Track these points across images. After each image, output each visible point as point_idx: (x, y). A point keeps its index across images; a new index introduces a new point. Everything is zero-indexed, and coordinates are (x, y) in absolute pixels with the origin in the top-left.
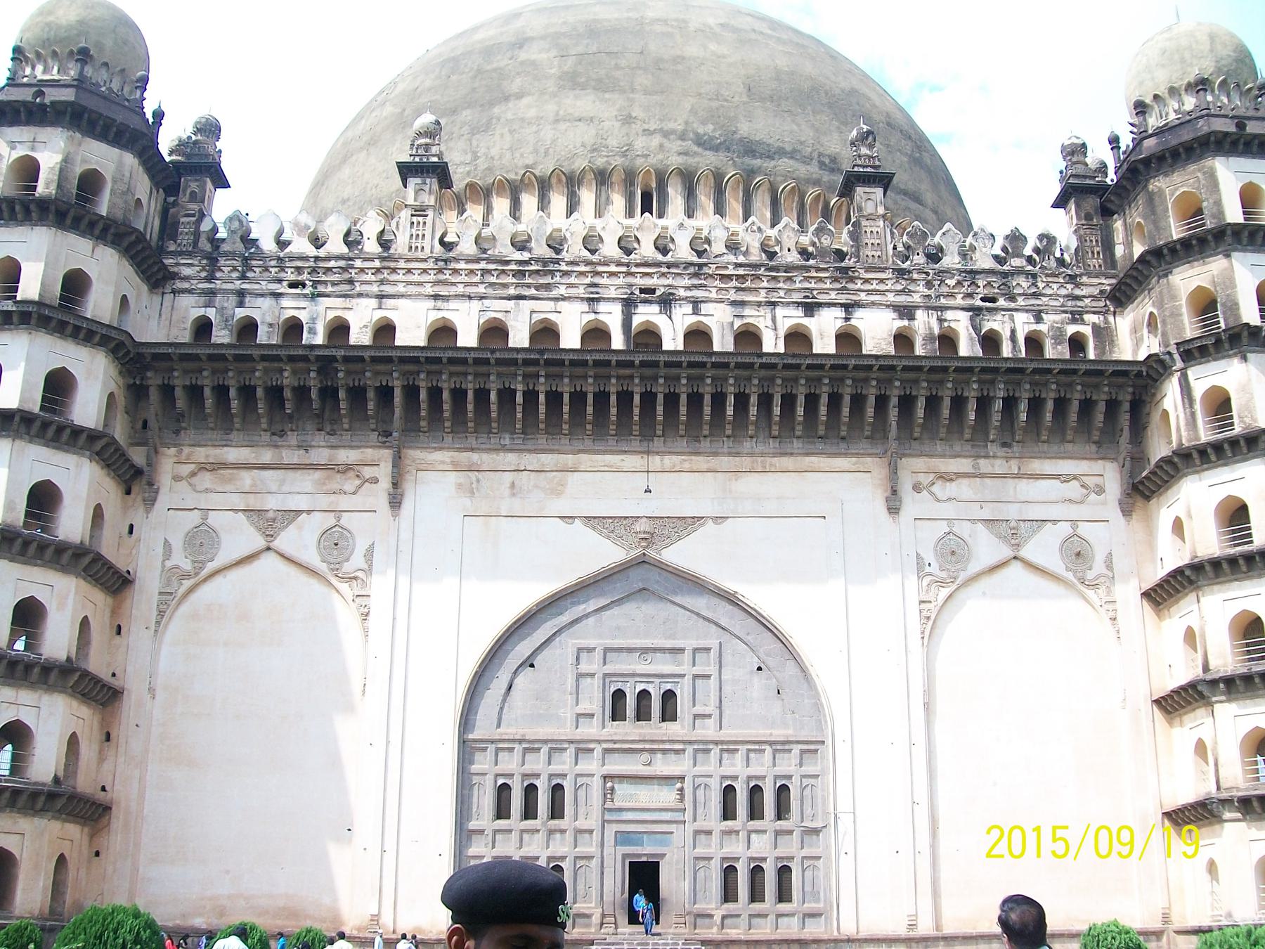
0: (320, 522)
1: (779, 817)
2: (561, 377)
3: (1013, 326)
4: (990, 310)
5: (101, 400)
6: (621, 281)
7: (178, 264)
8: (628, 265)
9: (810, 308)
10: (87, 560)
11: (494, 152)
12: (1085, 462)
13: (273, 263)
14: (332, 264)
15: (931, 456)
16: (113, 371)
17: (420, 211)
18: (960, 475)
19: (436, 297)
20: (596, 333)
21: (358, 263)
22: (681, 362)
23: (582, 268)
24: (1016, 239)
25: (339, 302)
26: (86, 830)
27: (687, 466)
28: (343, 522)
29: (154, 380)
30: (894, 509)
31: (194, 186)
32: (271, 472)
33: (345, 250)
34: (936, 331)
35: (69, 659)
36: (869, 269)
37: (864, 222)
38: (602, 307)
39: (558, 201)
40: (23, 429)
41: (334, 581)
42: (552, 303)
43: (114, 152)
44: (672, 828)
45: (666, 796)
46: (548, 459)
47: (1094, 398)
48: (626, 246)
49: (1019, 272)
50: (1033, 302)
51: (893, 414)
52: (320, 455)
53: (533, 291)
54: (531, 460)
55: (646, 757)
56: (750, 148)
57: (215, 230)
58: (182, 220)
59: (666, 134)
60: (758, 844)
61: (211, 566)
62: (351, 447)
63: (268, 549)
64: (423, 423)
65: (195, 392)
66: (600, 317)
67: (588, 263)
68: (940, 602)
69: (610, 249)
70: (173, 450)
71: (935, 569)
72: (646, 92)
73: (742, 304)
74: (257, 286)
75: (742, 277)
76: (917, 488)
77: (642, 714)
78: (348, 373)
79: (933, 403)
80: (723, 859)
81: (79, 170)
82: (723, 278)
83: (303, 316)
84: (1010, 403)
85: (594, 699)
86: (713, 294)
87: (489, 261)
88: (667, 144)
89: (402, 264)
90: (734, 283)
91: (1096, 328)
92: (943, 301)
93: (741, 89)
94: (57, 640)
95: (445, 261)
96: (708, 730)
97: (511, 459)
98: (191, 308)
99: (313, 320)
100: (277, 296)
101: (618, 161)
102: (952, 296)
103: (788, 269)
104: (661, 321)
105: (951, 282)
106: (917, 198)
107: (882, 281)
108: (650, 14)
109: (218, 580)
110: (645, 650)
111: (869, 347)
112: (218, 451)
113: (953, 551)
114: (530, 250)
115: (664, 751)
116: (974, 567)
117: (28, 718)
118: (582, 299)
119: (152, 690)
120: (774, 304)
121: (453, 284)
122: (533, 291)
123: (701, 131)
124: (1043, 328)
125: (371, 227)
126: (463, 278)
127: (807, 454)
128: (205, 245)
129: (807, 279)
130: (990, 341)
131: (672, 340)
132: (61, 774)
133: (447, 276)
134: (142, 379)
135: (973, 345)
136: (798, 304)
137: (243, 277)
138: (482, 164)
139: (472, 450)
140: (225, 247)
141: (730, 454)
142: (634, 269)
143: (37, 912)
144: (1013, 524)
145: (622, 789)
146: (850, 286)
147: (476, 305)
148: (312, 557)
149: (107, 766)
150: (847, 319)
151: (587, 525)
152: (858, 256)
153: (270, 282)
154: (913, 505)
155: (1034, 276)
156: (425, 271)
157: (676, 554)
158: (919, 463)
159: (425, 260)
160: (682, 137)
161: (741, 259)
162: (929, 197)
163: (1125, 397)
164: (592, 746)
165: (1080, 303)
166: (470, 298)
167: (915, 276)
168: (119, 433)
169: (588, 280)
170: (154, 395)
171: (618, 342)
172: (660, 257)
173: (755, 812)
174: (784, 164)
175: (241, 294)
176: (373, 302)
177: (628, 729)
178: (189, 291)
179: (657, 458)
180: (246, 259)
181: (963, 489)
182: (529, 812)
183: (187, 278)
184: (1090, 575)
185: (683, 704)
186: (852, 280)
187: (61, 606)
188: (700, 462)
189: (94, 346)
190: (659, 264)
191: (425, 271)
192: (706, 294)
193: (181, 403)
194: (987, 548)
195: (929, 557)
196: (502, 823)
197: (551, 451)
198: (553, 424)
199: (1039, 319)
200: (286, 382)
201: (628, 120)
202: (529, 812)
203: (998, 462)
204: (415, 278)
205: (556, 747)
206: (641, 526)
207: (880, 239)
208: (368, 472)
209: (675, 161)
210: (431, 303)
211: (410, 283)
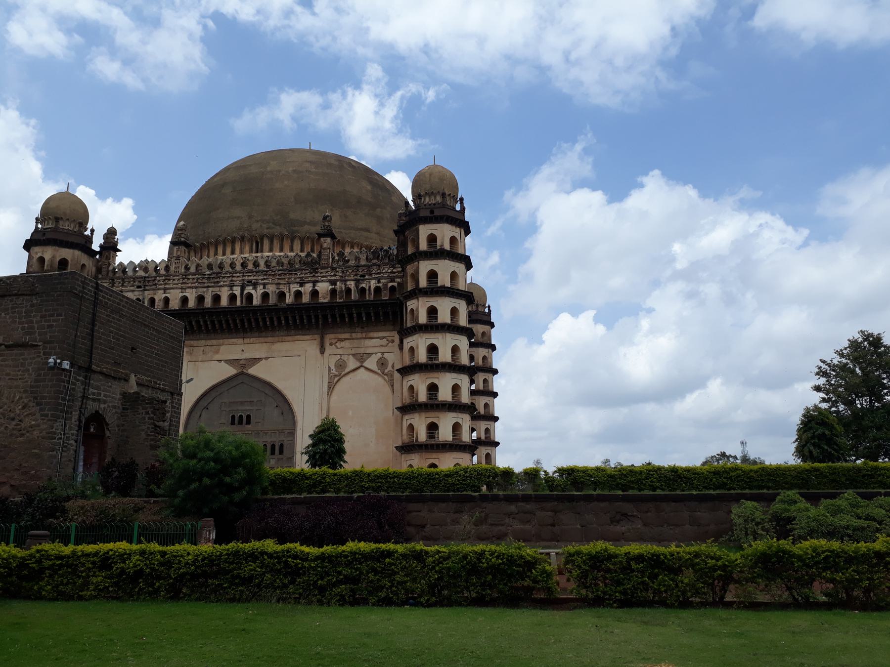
9: (302, 284)
18: (345, 339)
19: (182, 288)
20: (233, 297)
25: (152, 292)
30: (322, 352)
33: (154, 274)
38: (235, 288)
39: (229, 250)
42: (218, 289)
43: (71, 251)
46: (214, 342)
48: (244, 265)
49: (375, 264)
54: (210, 342)
57: (114, 269)
67: (230, 273)
69: (238, 267)
71: (334, 372)
73: (279, 284)
76: (331, 344)
77: (240, 422)
81: (58, 259)
82: (274, 275)
83: (141, 298)
84: (359, 316)
85: (227, 419)
97: (203, 342)
100: (133, 291)
102: (349, 276)
104: (253, 292)
106: (368, 230)
110: (242, 403)
113: (341, 365)
114: (212, 269)
116: (347, 370)
124: (380, 285)
128: (111, 274)
130: (363, 289)
133: (186, 280)
137: (122, 285)
140: (117, 275)
150: (314, 287)
154: (329, 350)
157: (252, 371)
158: (332, 336)
166: (192, 288)
174: (306, 228)
176: (162, 291)
181: (346, 344)
184: (386, 371)
186: (317, 273)
188: (262, 340)
190: (252, 272)
194: (352, 363)
195: (333, 367)
197: (215, 339)
198: (215, 331)
199: (379, 282)
201: (250, 217)
204: (176, 282)
206: (241, 362)
209: (266, 232)
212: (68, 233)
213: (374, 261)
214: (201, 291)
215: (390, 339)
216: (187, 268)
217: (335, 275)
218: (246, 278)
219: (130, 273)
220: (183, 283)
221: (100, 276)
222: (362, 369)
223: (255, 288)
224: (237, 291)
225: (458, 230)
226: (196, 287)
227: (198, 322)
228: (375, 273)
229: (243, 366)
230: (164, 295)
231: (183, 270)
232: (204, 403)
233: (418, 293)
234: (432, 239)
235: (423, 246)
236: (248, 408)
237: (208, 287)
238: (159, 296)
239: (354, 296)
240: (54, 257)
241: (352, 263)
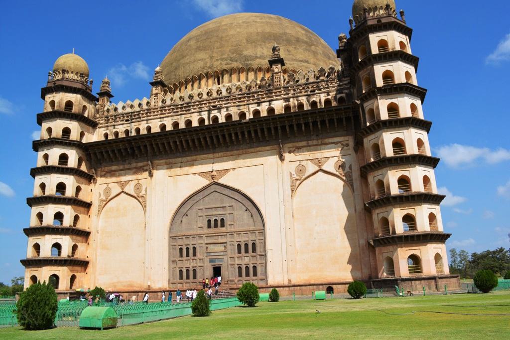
0: (133, 184)
1: (253, 252)
2: (187, 136)
3: (321, 98)
4: (313, 95)
5: (75, 159)
6: (208, 105)
7: (99, 121)
8: (209, 100)
9: (259, 104)
10: (72, 201)
11: (180, 73)
12: (342, 137)
14: (135, 113)
15: (294, 142)
16: (79, 151)
17: (156, 95)
19: (160, 118)
20: (202, 121)
21: (142, 112)
22: (333, 110)
23: (197, 103)
24: (322, 71)
26: (83, 268)
27: (225, 155)
28: (139, 182)
32: (122, 172)
34: (296, 104)
35: (70, 226)
36: (275, 89)
37: (275, 75)
38: (202, 113)
40: (54, 170)
41: (138, 198)
42: (189, 115)
44: (223, 257)
45: (221, 248)
46: (189, 158)
47: (341, 117)
49: (322, 81)
50: (326, 90)
51: (280, 131)
52: (134, 165)
53: (185, 112)
54: (185, 159)
55: (216, 238)
56: (247, 58)
59: (222, 59)
60: (246, 260)
61: (110, 198)
62: (141, 162)
63: (123, 192)
64: (157, 153)
66: (202, 116)
67: (199, 102)
68: (297, 186)
69: (205, 96)
70: (100, 169)
71: (295, 176)
72: (217, 48)
73: (240, 106)
75: (240, 98)
76: (290, 152)
77: (216, 226)
78: (135, 143)
79: (291, 127)
80: (238, 265)
81: (65, 101)
82: (236, 99)
83: (129, 129)
86: (232, 104)
87: (173, 106)
88: (222, 62)
89: (152, 110)
90: (238, 100)
91: (346, 94)
92: (298, 94)
93: (245, 41)
94: (67, 222)
95: (163, 108)
96: (232, 229)
97: (180, 159)
99: (131, 129)
101: (209, 70)
102: (301, 92)
103: (253, 93)
104: (218, 115)
105: (301, 88)
106: (307, 62)
107: (280, 92)
108: (223, 23)
109: (112, 201)
111: (277, 112)
112: (110, 168)
113: (301, 170)
114: (183, 100)
115: (221, 235)
116: (307, 174)
117: (59, 242)
118: (197, 112)
119: (97, 231)
120: (249, 104)
121: (165, 114)
122: (185, 112)
123: (232, 56)
124: (329, 97)
125: (144, 101)
126: (168, 111)
127: (257, 147)
128: (106, 114)
129: (258, 95)
130: (314, 104)
131: (222, 120)
132: (70, 255)
135: (307, 106)
136: (255, 103)
137: (115, 121)
138: (178, 77)
139: (170, 158)
141: (236, 150)
142: (210, 101)
143: (65, 289)
144: (319, 159)
145: (211, 247)
146: (271, 95)
147: (170, 118)
148: (133, 193)
149: (88, 251)
150: (270, 105)
151: (199, 175)
152: (273, 86)
153: (121, 121)
155: (327, 81)
156: (158, 112)
158: (290, 145)
159: (157, 109)
160: (226, 60)
161: (240, 93)
162: (312, 61)
163: (351, 115)
164: (202, 235)
165: (342, 87)
167: (290, 88)
168: (83, 168)
169: (199, 106)
170: (92, 156)
171: (207, 123)
172: (218, 96)
173: (247, 251)
174: (258, 61)
175: (114, 126)
176: (145, 122)
177: (212, 230)
178: (102, 127)
179: (217, 154)
180: (115, 116)
182: (188, 255)
185: (227, 223)
186: (271, 93)
187: (67, 213)
188: (228, 153)
189: (72, 146)
190: (217, 99)
191: (158, 112)
192: (230, 105)
193: (99, 157)
194: (311, 168)
195: (293, 173)
196: (181, 259)
199: (328, 95)
200: (121, 148)
201: (212, 58)
202: (188, 255)
203: (314, 141)
204: (156, 113)
205: (193, 236)
206: (214, 173)
207: (282, 79)
208: (145, 168)
209: (225, 67)
210: (159, 120)
211: (154, 116)
212: (73, 81)
213: (322, 78)
214: (175, 119)
215: (344, 143)
216: (163, 101)
217: (288, 94)
218: (212, 104)
219: (120, 111)
220: (161, 114)
221: (98, 116)
222: (320, 173)
223: (219, 112)
224: (205, 115)
225: (404, 36)
226: (172, 116)
227: (175, 142)
228: (324, 88)
229: (213, 177)
230: (147, 125)
231: (160, 104)
232: (183, 210)
233: (374, 92)
234: (383, 44)
235: (375, 50)
236: (221, 213)
237: (181, 114)
238: (143, 127)
239: (307, 107)
241: (302, 81)
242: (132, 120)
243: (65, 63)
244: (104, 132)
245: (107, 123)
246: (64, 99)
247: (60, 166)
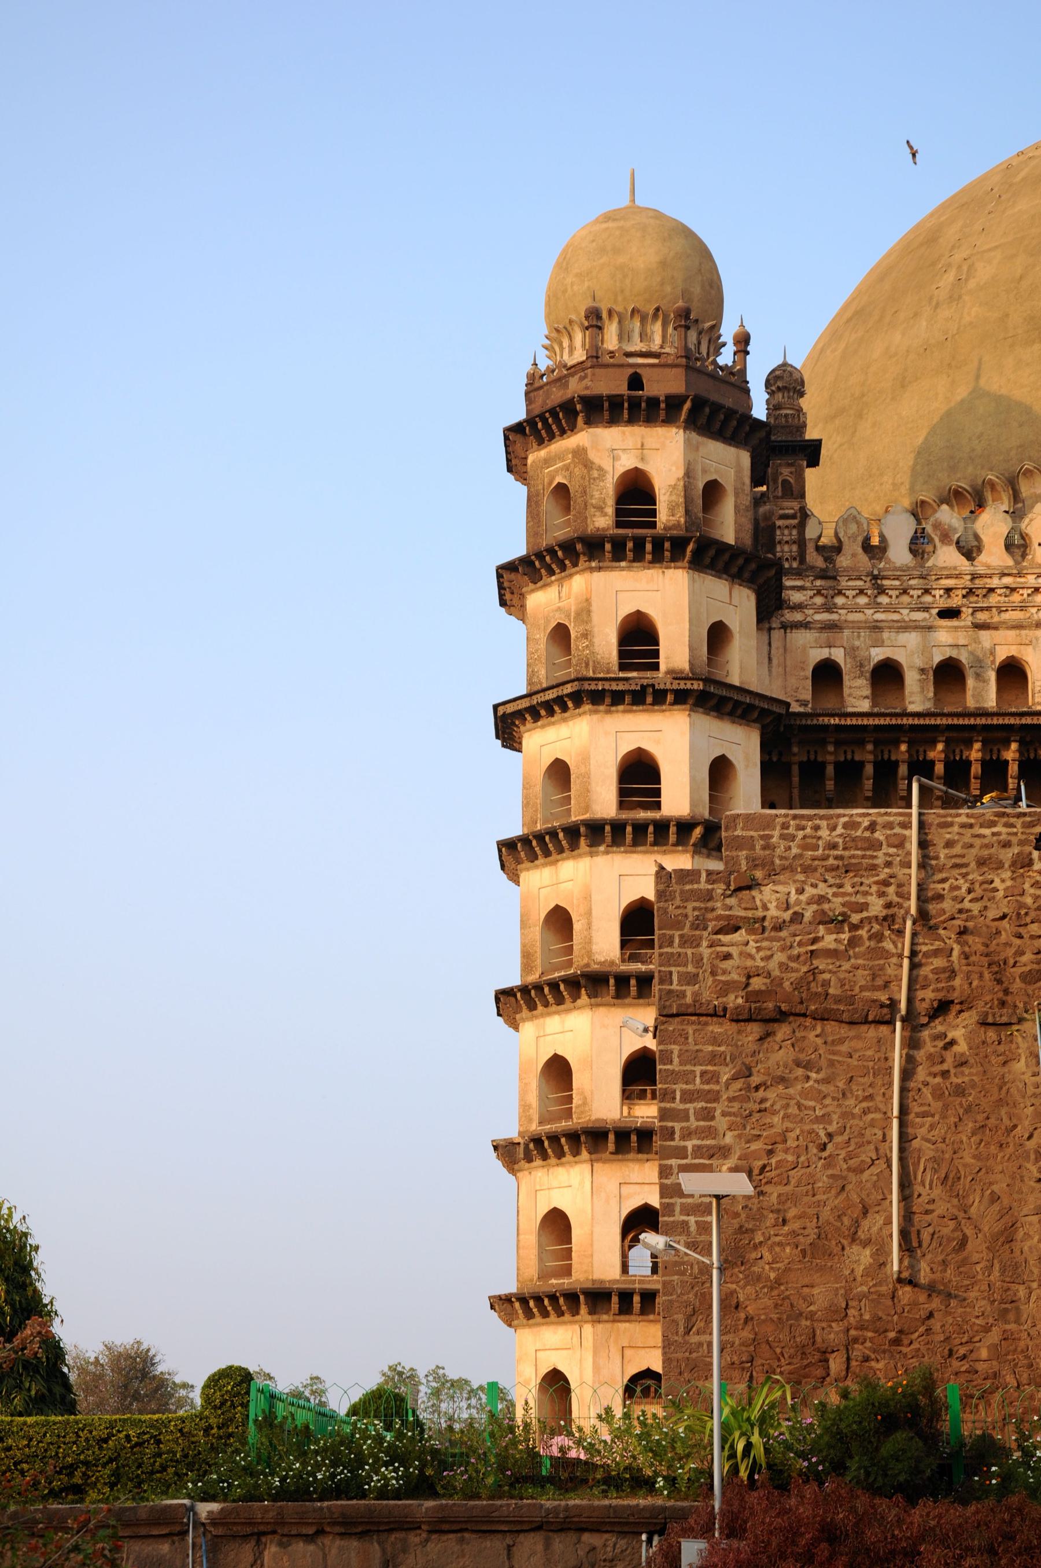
13: (912, 582)
29: (798, 754)
31: (786, 472)
33: (1010, 562)
58: (779, 523)
65: (849, 772)
74: (895, 617)
81: (701, 486)
83: (964, 658)
98: (811, 649)
128: (815, 560)
134: (780, 754)
153: (912, 610)
175: (876, 627)
178: (805, 625)
180: (875, 578)
183: (799, 607)
240: (689, 474)
242: (976, 610)
243: (663, 264)
244: (818, 655)
245: (829, 608)
246: (699, 468)
247: (625, 815)
